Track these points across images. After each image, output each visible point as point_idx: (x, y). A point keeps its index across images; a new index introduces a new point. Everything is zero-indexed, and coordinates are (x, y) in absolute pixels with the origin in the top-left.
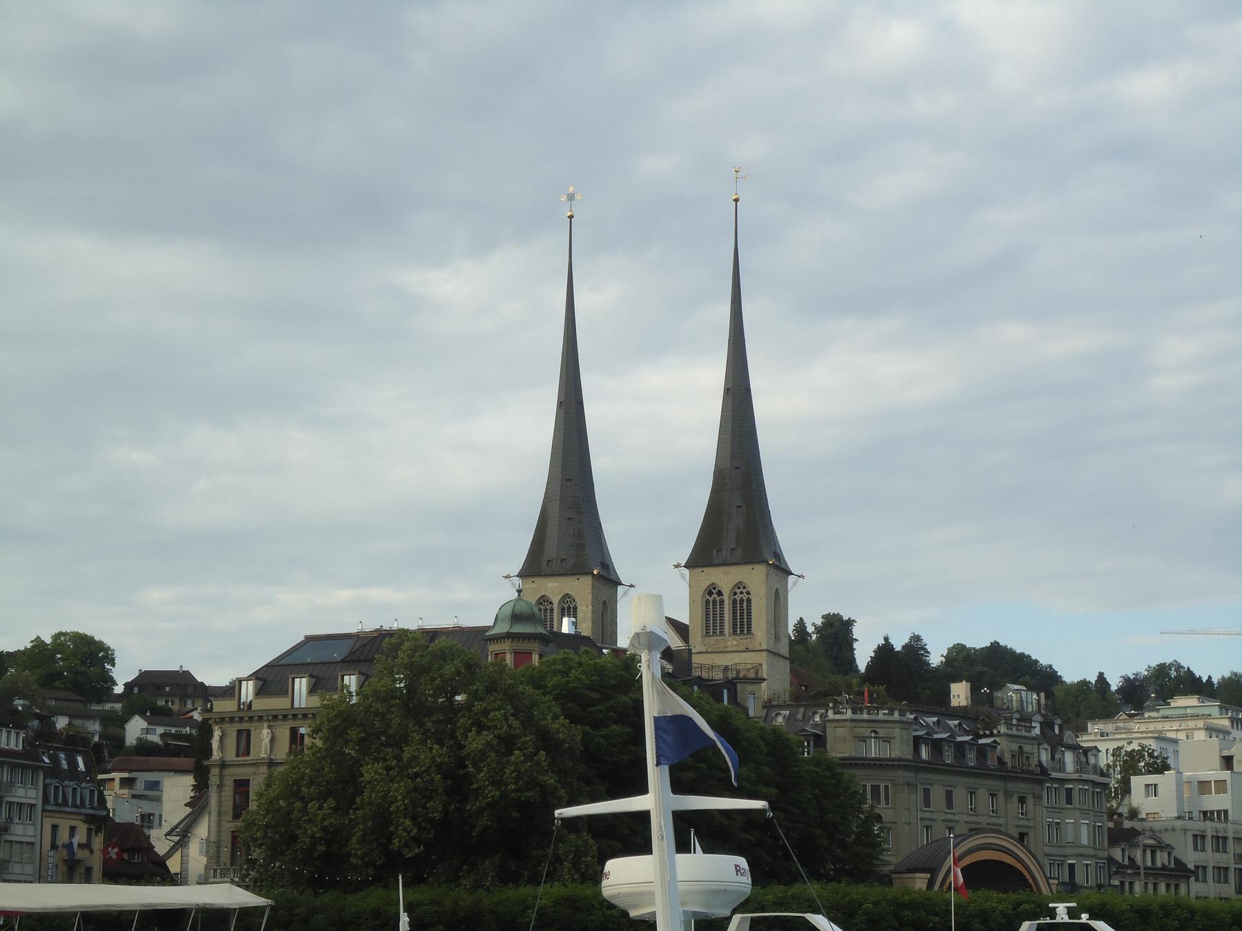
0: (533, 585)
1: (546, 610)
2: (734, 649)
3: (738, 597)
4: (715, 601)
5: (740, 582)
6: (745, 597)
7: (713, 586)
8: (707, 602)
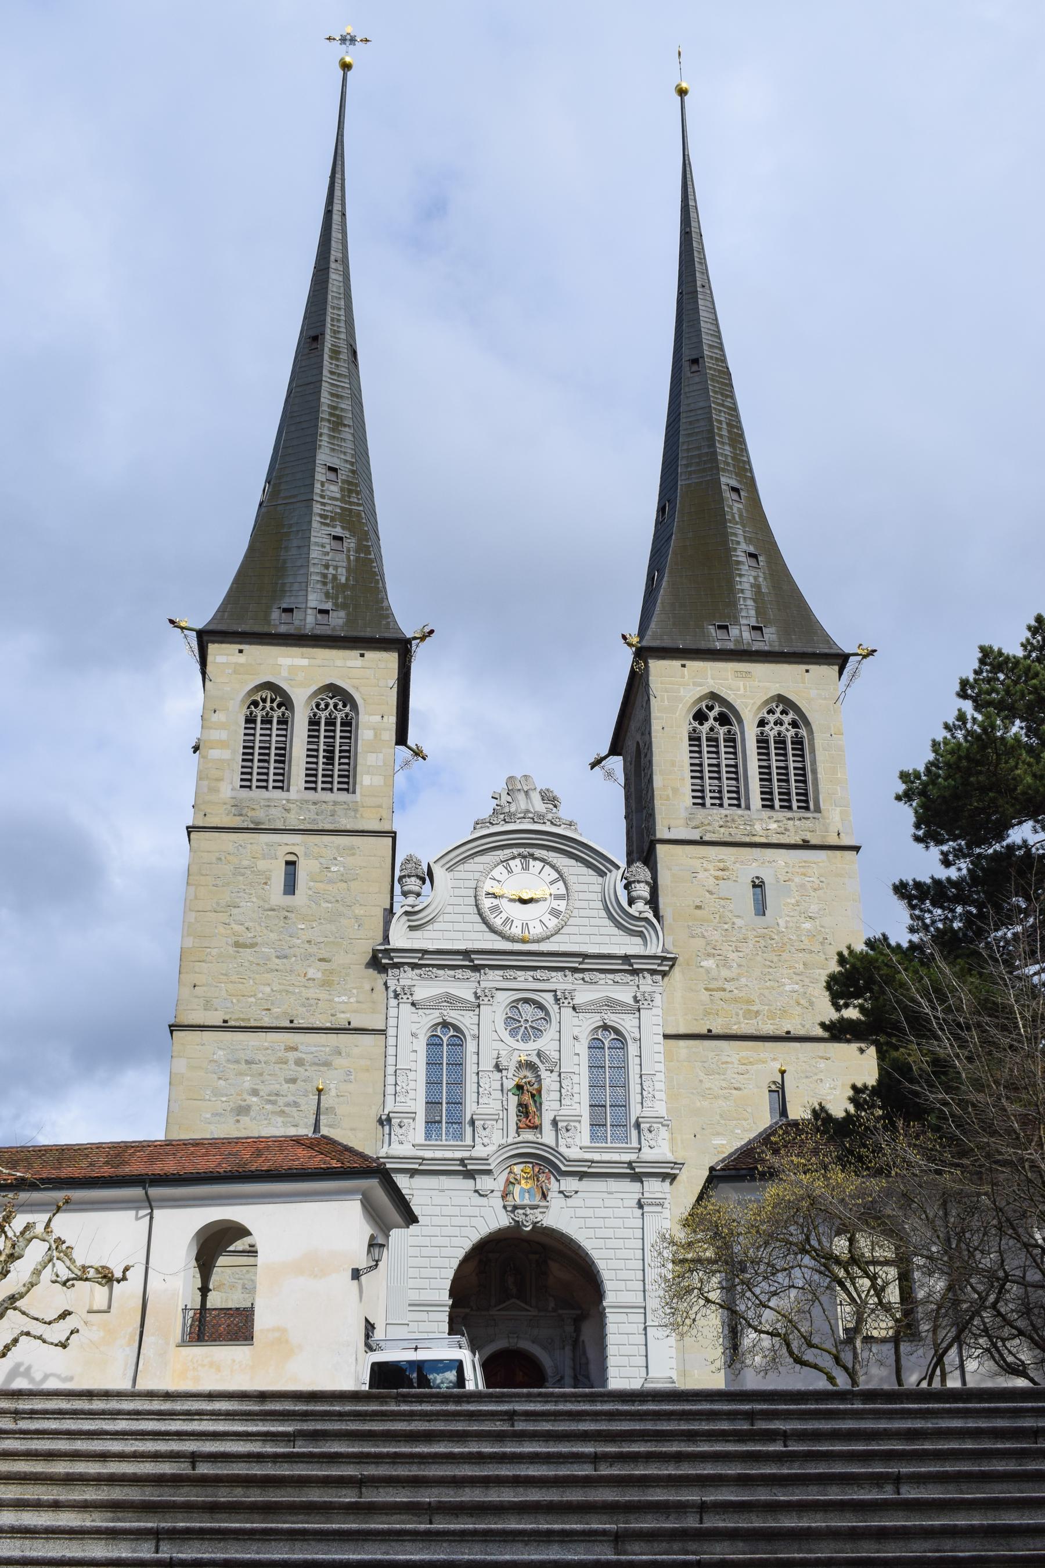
0: (241, 659)
1: (267, 721)
2: (774, 840)
4: (713, 740)
5: (781, 699)
8: (694, 739)
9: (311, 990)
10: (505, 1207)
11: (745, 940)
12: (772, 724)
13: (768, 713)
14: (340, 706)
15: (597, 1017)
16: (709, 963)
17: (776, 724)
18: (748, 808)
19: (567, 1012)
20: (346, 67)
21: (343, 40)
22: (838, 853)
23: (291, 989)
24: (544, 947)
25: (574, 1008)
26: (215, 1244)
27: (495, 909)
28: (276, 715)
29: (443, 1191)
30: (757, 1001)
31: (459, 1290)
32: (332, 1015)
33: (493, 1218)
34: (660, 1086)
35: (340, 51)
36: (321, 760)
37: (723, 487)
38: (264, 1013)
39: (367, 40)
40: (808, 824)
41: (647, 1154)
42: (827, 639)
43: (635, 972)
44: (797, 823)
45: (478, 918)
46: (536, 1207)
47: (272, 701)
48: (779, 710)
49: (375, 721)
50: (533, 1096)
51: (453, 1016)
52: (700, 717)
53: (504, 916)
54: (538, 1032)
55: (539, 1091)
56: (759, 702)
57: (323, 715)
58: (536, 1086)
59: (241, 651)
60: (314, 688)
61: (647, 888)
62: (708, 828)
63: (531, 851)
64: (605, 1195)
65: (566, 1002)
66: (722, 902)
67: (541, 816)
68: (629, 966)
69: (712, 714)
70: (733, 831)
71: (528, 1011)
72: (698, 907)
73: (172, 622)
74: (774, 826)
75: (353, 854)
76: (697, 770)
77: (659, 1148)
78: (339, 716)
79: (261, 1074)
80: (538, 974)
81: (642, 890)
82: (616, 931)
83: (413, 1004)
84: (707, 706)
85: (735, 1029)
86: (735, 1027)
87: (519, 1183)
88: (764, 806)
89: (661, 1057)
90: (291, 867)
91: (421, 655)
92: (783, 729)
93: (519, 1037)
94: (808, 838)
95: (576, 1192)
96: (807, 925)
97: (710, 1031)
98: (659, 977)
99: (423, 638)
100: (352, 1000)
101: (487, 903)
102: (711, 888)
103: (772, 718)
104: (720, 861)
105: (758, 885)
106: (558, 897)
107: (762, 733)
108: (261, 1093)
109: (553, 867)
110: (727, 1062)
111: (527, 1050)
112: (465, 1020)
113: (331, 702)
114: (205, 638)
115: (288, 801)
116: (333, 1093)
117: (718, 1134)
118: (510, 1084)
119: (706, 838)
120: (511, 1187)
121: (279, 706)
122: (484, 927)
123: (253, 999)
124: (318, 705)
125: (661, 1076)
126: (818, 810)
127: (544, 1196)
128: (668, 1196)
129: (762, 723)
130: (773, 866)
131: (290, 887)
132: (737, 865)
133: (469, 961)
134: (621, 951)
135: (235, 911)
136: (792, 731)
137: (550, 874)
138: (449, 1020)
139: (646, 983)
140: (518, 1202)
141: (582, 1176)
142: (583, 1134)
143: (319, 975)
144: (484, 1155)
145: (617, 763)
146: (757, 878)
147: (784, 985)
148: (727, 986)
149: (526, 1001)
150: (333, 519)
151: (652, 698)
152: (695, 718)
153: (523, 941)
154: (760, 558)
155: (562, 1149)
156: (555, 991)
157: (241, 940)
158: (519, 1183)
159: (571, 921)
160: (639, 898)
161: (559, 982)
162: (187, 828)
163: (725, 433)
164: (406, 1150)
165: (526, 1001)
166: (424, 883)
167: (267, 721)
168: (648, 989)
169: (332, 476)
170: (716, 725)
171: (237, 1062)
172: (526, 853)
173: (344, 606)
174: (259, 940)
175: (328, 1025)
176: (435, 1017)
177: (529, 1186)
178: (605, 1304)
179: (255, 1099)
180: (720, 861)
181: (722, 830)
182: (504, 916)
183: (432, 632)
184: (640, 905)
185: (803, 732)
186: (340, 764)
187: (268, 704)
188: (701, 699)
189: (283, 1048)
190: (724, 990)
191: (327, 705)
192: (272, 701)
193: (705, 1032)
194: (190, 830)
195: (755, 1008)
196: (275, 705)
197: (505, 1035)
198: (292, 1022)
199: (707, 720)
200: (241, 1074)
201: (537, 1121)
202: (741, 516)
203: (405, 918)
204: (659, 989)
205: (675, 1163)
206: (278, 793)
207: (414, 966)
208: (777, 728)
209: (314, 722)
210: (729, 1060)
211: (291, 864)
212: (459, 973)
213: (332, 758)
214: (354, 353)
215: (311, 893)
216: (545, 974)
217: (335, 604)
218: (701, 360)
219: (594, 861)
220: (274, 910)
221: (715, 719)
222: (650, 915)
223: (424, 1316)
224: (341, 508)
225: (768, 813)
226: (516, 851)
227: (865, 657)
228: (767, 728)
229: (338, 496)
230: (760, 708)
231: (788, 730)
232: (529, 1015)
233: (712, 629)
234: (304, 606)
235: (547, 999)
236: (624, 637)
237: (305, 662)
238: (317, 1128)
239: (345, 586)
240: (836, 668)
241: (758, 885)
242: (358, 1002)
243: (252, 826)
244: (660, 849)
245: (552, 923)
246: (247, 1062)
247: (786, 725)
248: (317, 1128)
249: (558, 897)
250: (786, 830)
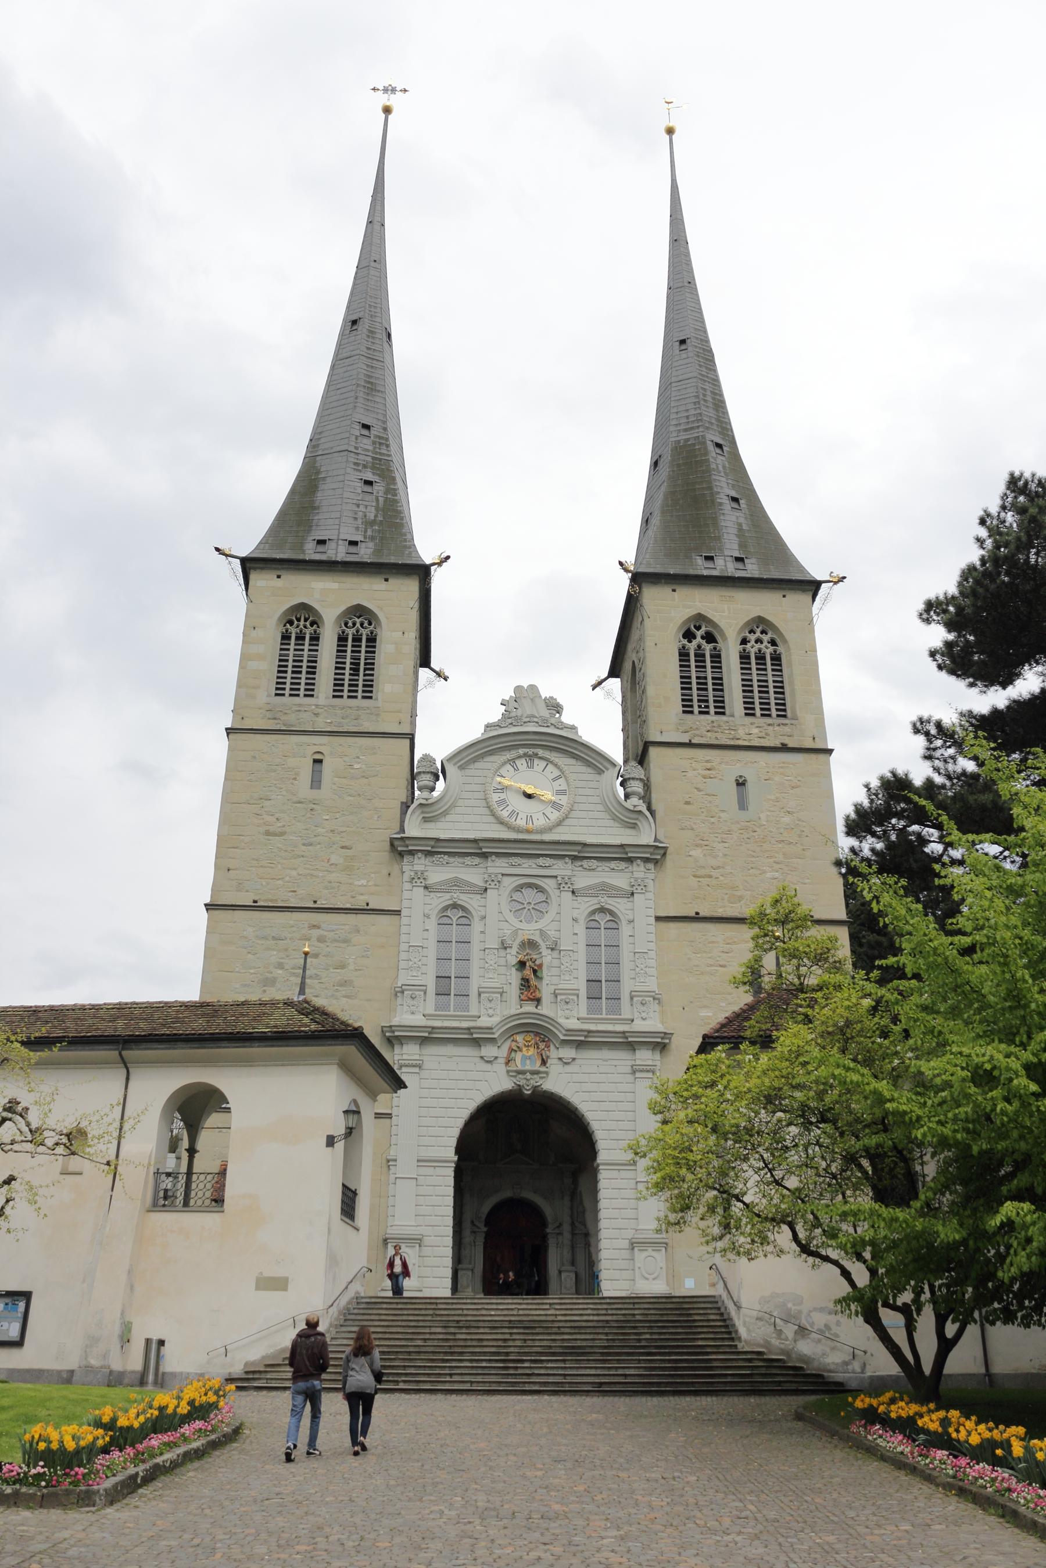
0: (279, 583)
1: (300, 638)
2: (756, 742)
3: (752, 649)
4: (700, 656)
5: (760, 620)
6: (768, 651)
7: (700, 619)
8: (683, 655)
9: (334, 874)
10: (508, 1072)
11: (729, 832)
12: (752, 642)
13: (750, 632)
14: (366, 624)
15: (595, 900)
16: (697, 853)
17: (756, 642)
18: (733, 716)
20: (387, 110)
21: (385, 90)
22: (813, 756)
23: (315, 873)
24: (547, 837)
25: (573, 892)
26: (195, 1108)
27: (502, 802)
28: (308, 632)
29: (450, 1057)
30: (741, 887)
31: (466, 1146)
32: (353, 897)
33: (496, 1082)
34: (652, 963)
35: (383, 99)
36: (347, 672)
37: (709, 443)
38: (291, 894)
39: (405, 91)
40: (787, 729)
41: (639, 1026)
42: (801, 569)
43: (630, 860)
44: (777, 728)
45: (487, 811)
46: (537, 1073)
47: (306, 620)
48: (758, 631)
49: (395, 641)
50: (535, 971)
51: (464, 899)
52: (689, 635)
53: (510, 809)
55: (540, 966)
56: (742, 623)
57: (350, 632)
58: (537, 962)
59: (279, 577)
60: (343, 608)
61: (641, 785)
62: (696, 732)
63: (535, 751)
64: (600, 1062)
65: (566, 887)
66: (710, 798)
67: (545, 720)
68: (624, 855)
69: (699, 634)
70: (719, 735)
71: (529, 895)
72: (687, 803)
73: (217, 549)
74: (755, 731)
75: (375, 754)
76: (685, 683)
77: (649, 1022)
78: (364, 633)
79: (286, 950)
80: (541, 861)
81: (637, 787)
82: (611, 823)
83: (426, 887)
84: (695, 627)
85: (720, 912)
86: (720, 910)
87: (521, 1050)
88: (746, 714)
89: (652, 937)
90: (317, 765)
91: (438, 577)
92: (762, 646)
93: (522, 918)
94: (786, 742)
95: (574, 1059)
96: (787, 819)
97: (697, 913)
98: (651, 866)
99: (440, 564)
100: (370, 883)
101: (495, 797)
102: (698, 786)
103: (752, 637)
104: (708, 761)
105: (741, 783)
106: (560, 792)
107: (744, 650)
108: (286, 967)
109: (556, 765)
110: (713, 942)
111: (529, 930)
112: (472, 902)
113: (358, 621)
114: (249, 565)
115: (317, 706)
116: (351, 967)
117: (705, 1007)
118: (514, 961)
119: (693, 741)
120: (513, 1054)
121: (312, 625)
122: (492, 819)
123: (280, 882)
124: (346, 624)
125: (652, 954)
126: (795, 718)
127: (544, 1062)
128: (658, 1063)
129: (744, 641)
130: (754, 767)
131: (316, 782)
132: (723, 766)
133: (479, 850)
134: (617, 841)
135: (267, 803)
136: (771, 649)
137: (552, 771)
138: (460, 902)
139: (639, 870)
140: (520, 1067)
141: (580, 1045)
142: (582, 1008)
143: (341, 861)
144: (489, 1025)
145: (615, 683)
146: (741, 777)
147: (765, 872)
148: (714, 873)
149: (530, 886)
150: (365, 466)
151: (646, 618)
152: (684, 636)
153: (528, 831)
154: (741, 502)
155: (561, 1021)
156: (556, 877)
157: (272, 829)
158: (521, 1050)
159: (573, 814)
160: (634, 793)
161: (562, 868)
162: (227, 729)
163: (709, 398)
164: (418, 1020)
165: (530, 886)
166: (438, 779)
167: (300, 638)
168: (641, 875)
169: (365, 432)
170: (704, 642)
171: (265, 938)
172: (530, 753)
173: (372, 538)
174: (287, 829)
175: (348, 906)
176: (445, 899)
177: (530, 1053)
178: (598, 1161)
179: (280, 972)
180: (708, 761)
181: (709, 734)
182: (510, 809)
183: (448, 557)
184: (634, 801)
185: (780, 649)
186: (365, 675)
187: (302, 623)
188: (689, 620)
189: (306, 925)
190: (710, 877)
191: (354, 624)
192: (306, 620)
193: (693, 914)
194: (229, 731)
195: (739, 893)
196: (308, 623)
197: (510, 917)
198: (315, 902)
199: (695, 638)
200: (268, 949)
201: (538, 995)
202: (724, 467)
203: (419, 811)
204: (652, 876)
205: (665, 1033)
206: (308, 700)
207: (429, 854)
208: (758, 646)
209: (342, 639)
210: (713, 939)
212: (468, 860)
213: (358, 670)
214: (389, 336)
215: (334, 787)
216: (548, 861)
217: (365, 537)
218: (688, 341)
220: (300, 802)
221: (702, 638)
222: (644, 809)
223: (430, 1171)
224: (373, 458)
225: (750, 719)
226: (521, 751)
227: (836, 583)
228: (749, 645)
229: (371, 448)
230: (742, 629)
231: (767, 648)
233: (700, 561)
234: (335, 537)
235: (549, 885)
236: (621, 563)
237: (334, 586)
238: (302, 991)
239: (372, 523)
240: (811, 594)
241: (741, 783)
242: (376, 885)
243: (284, 728)
244: (653, 751)
245: (554, 816)
246: (274, 938)
247: (765, 643)
248: (302, 991)
249: (560, 792)
250: (767, 734)
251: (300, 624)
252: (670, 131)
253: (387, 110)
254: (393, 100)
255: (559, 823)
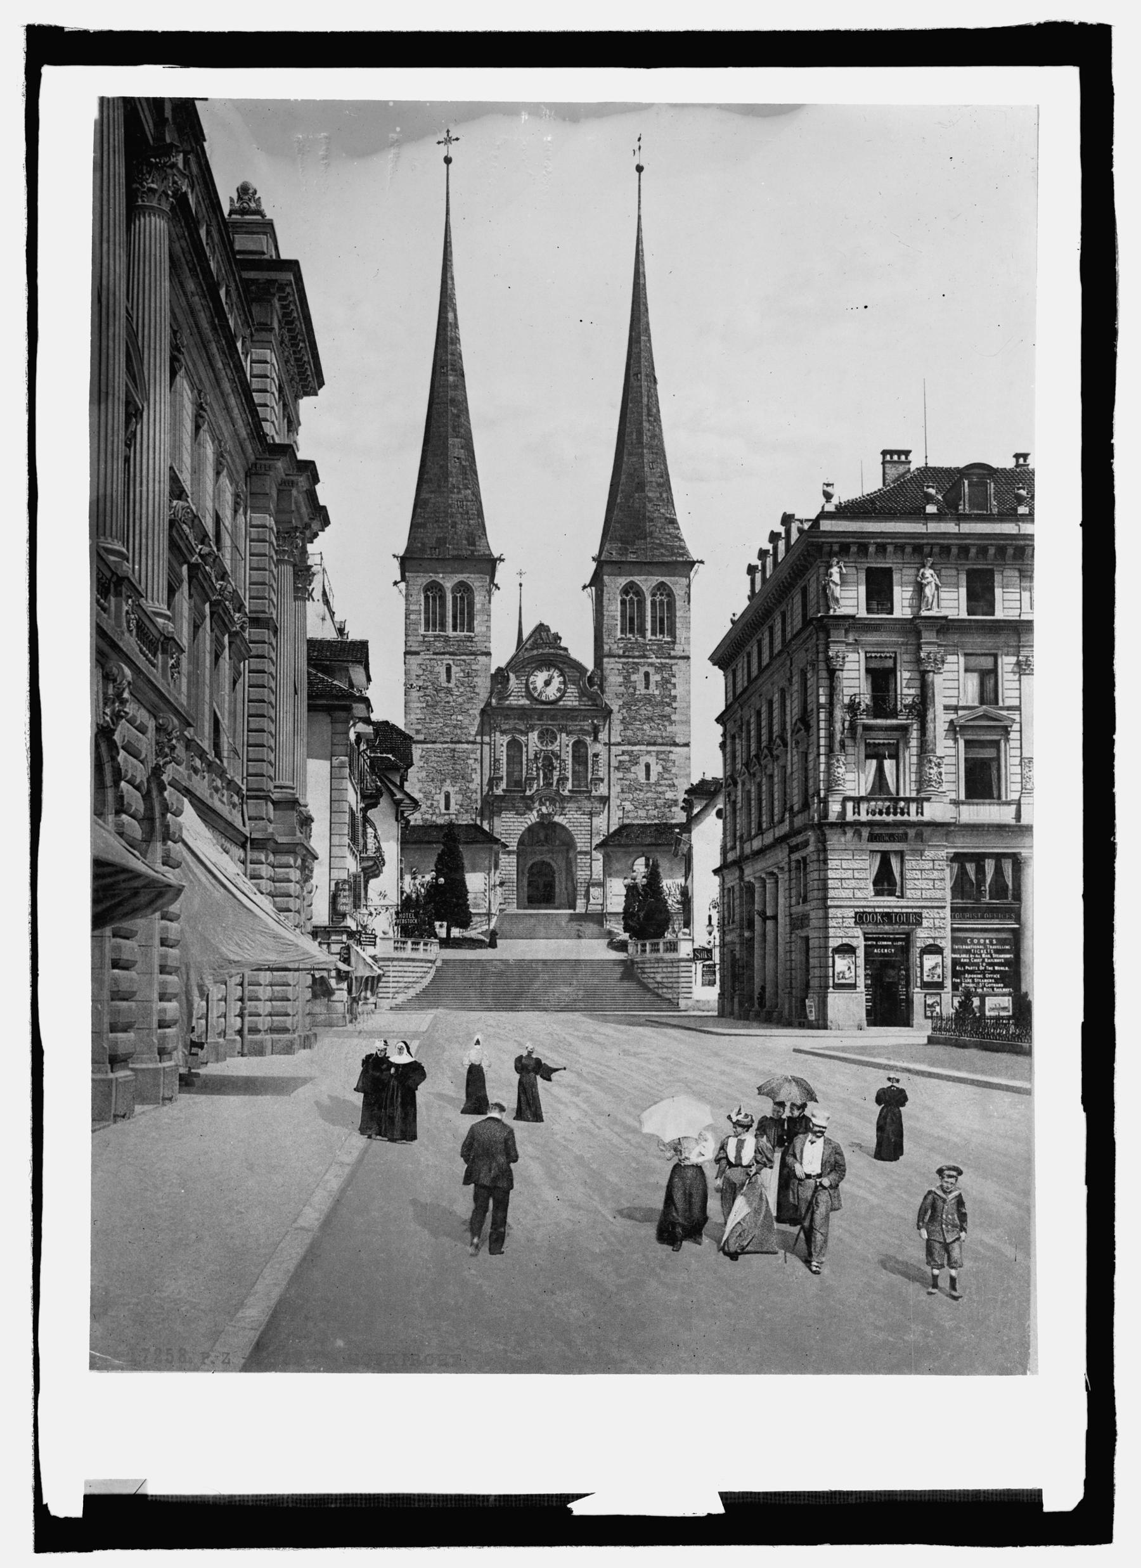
3: (658, 598)
19: (564, 735)
20: (448, 160)
54: (552, 743)
129: (654, 595)
133: (522, 713)
209: (454, 598)
211: (448, 669)
219: (578, 667)
232: (547, 736)
251: (434, 591)
252: (640, 169)
253: (448, 160)
254: (453, 150)
255: (560, 699)
